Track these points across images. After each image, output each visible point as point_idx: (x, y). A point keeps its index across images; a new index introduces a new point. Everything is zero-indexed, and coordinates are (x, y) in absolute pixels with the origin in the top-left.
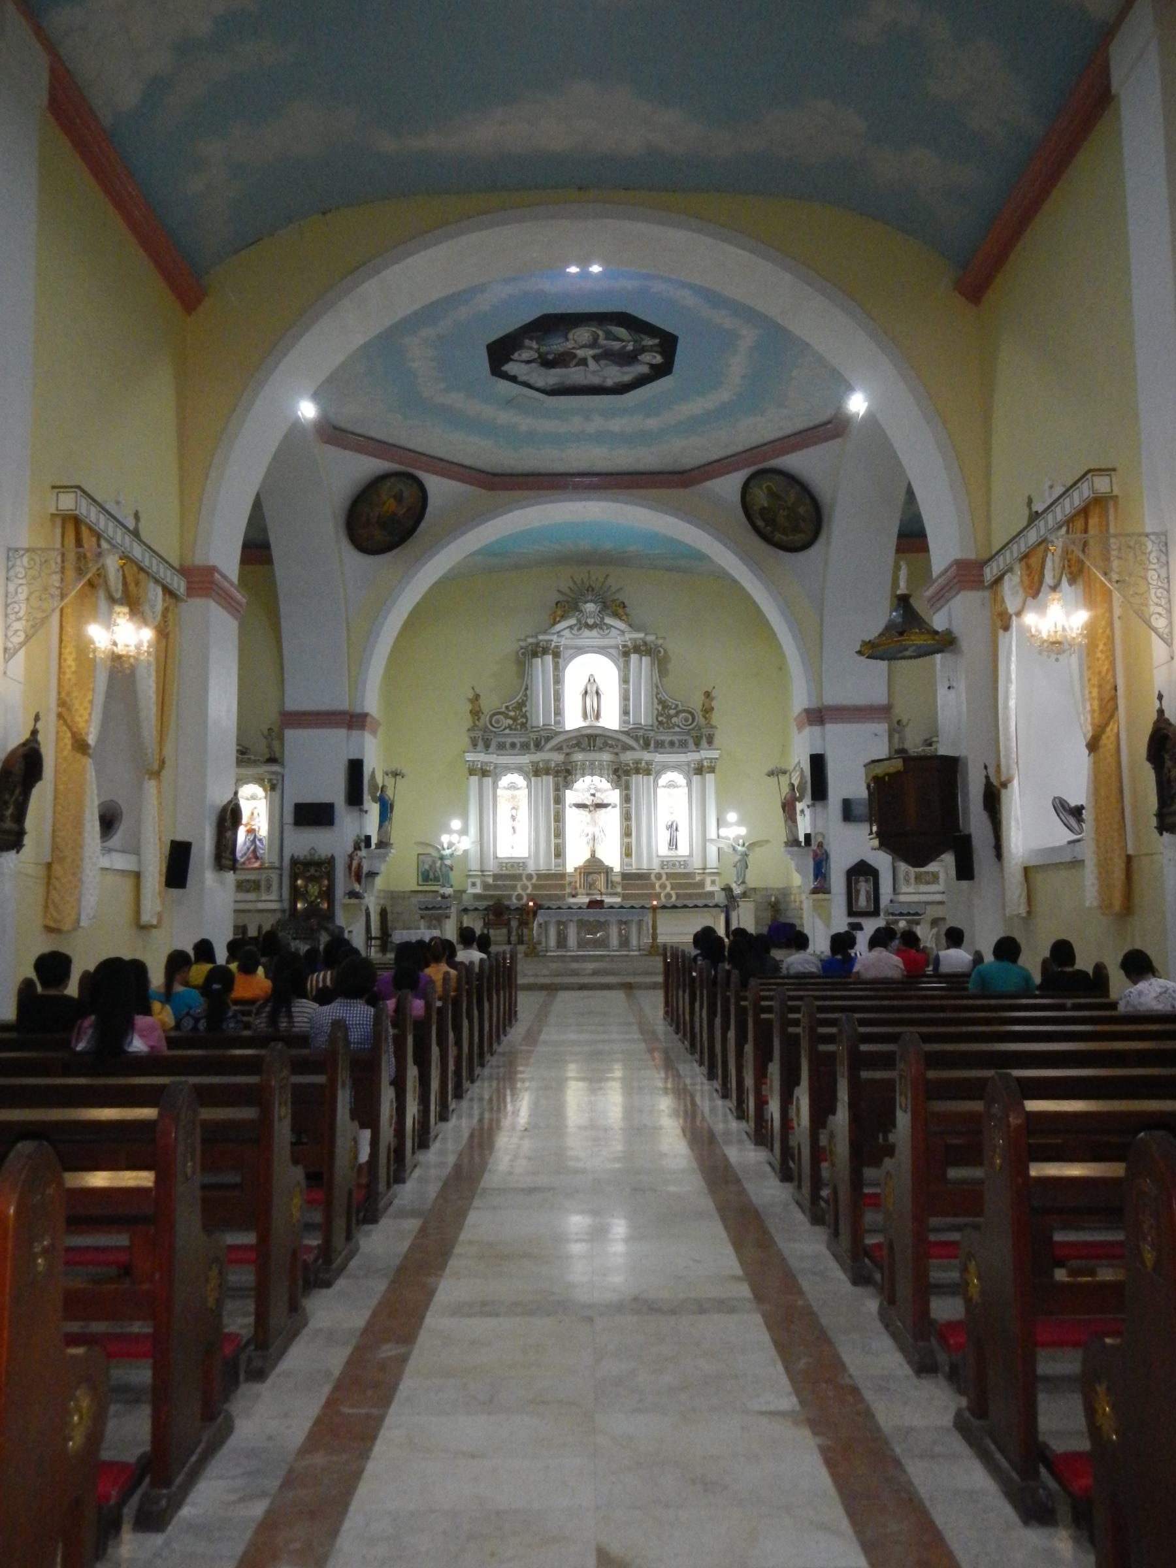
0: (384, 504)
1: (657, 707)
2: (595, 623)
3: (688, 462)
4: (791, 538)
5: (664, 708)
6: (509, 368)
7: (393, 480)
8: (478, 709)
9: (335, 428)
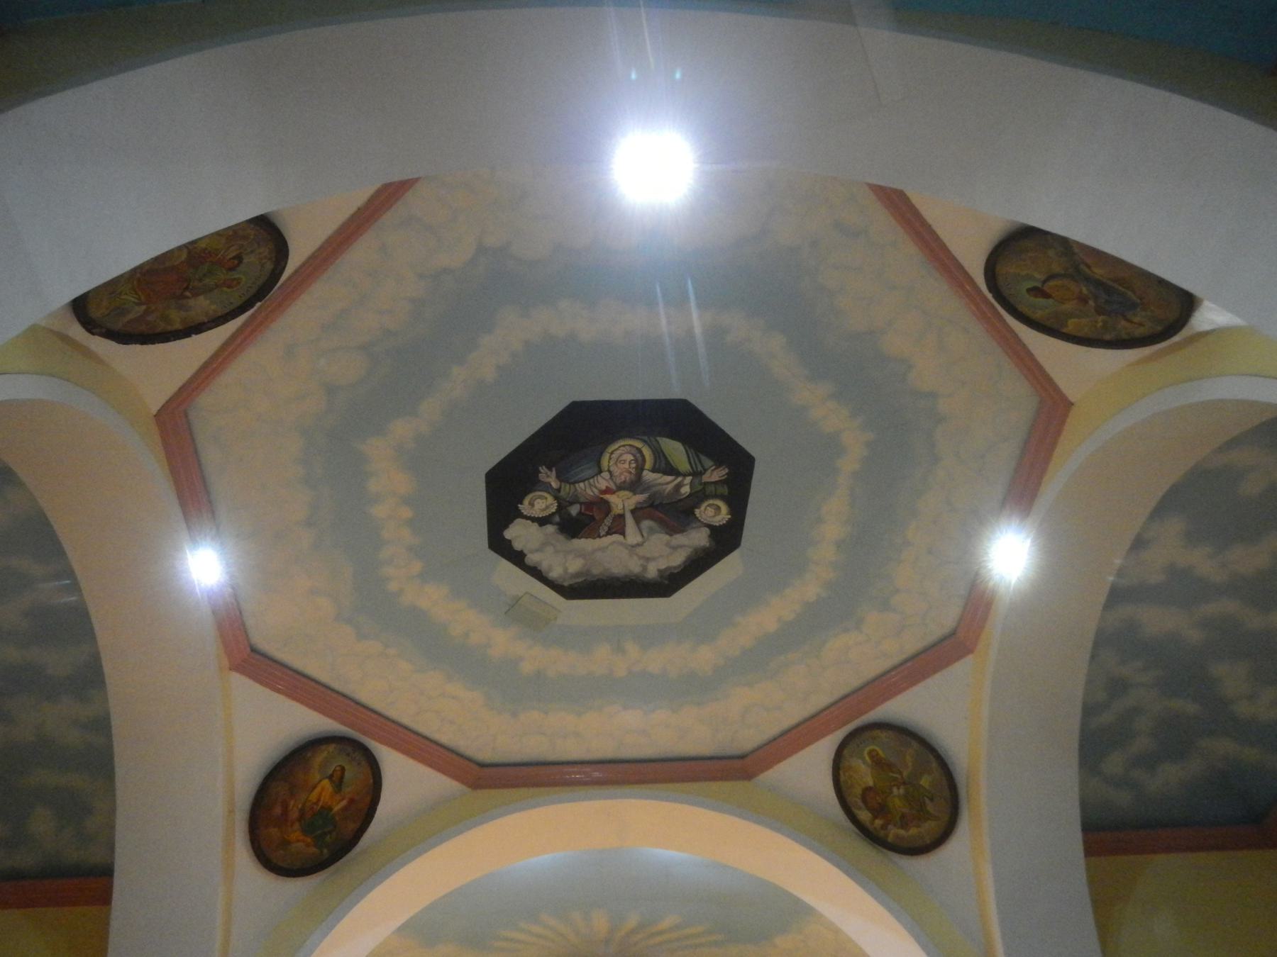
0: (314, 787)
3: (749, 738)
4: (913, 831)
6: (518, 533)
7: (331, 748)
9: (254, 650)
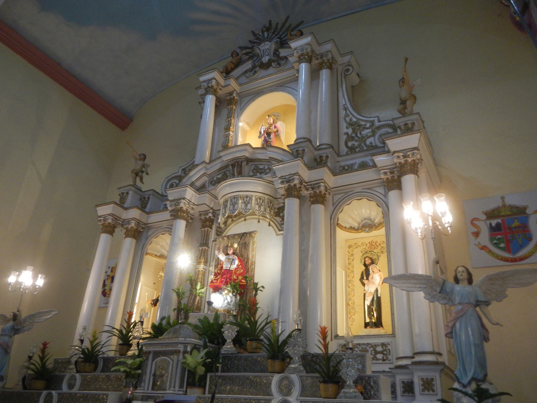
1: (346, 130)
2: (269, 60)
5: (354, 131)
8: (138, 167)
